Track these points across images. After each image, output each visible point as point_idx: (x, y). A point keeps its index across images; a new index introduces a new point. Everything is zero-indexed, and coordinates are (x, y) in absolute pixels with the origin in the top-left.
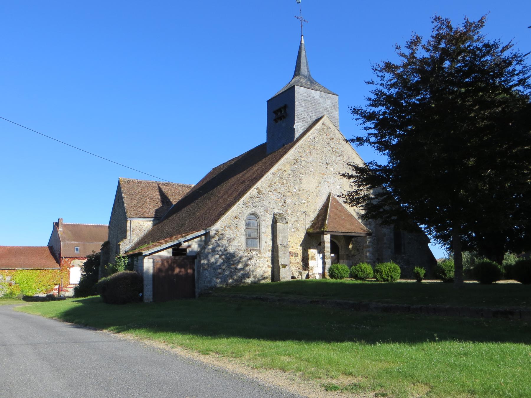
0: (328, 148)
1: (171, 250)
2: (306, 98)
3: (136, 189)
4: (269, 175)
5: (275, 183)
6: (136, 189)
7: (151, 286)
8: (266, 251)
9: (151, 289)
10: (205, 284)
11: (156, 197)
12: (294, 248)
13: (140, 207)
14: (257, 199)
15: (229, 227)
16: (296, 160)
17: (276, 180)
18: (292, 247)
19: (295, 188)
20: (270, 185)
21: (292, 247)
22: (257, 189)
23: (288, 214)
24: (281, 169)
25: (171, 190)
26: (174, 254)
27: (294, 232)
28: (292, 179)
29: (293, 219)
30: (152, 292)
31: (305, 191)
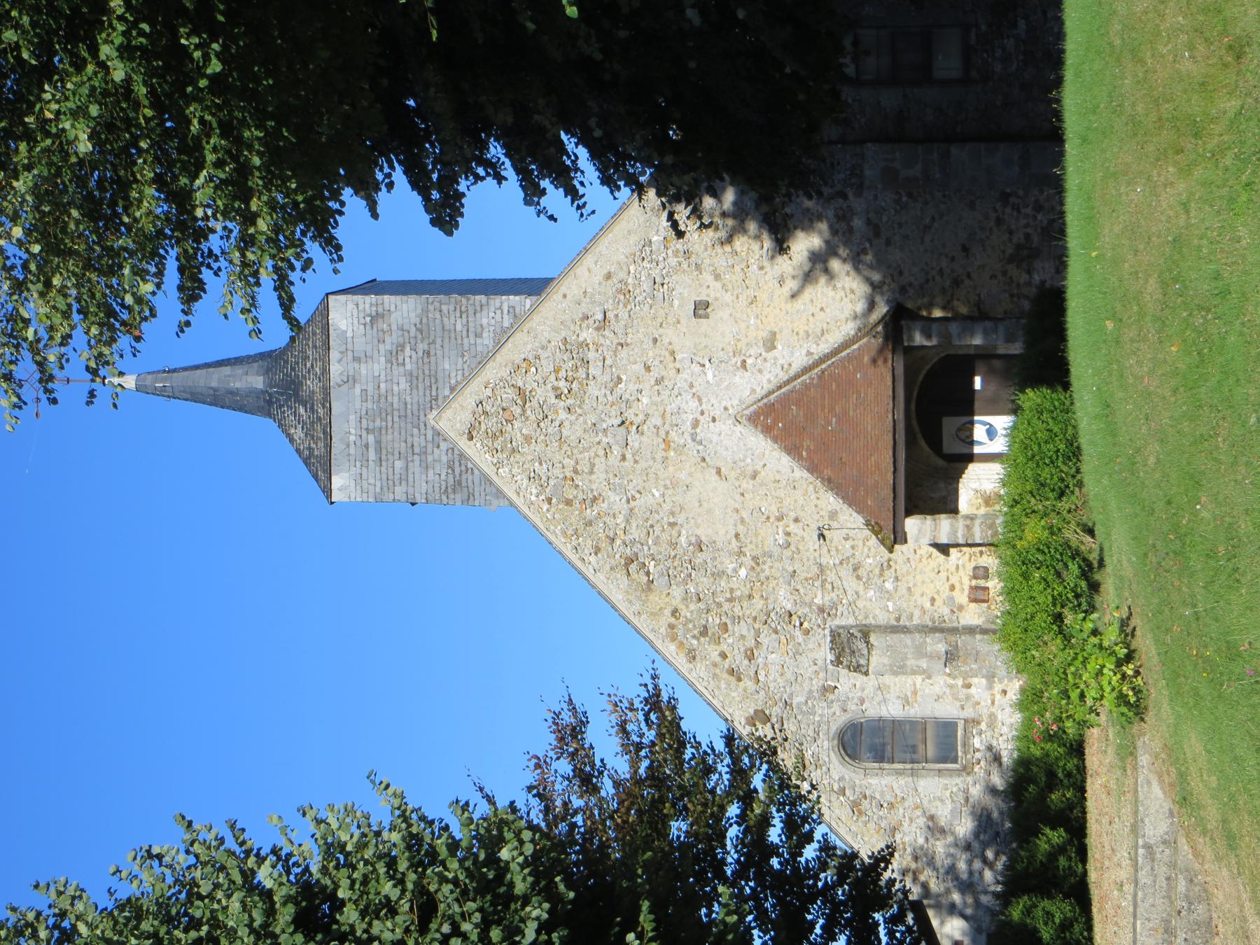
5: (724, 656)
8: (968, 697)
12: (954, 580)
16: (629, 561)
18: (952, 588)
21: (952, 588)
24: (671, 626)
27: (897, 579)
28: (703, 583)
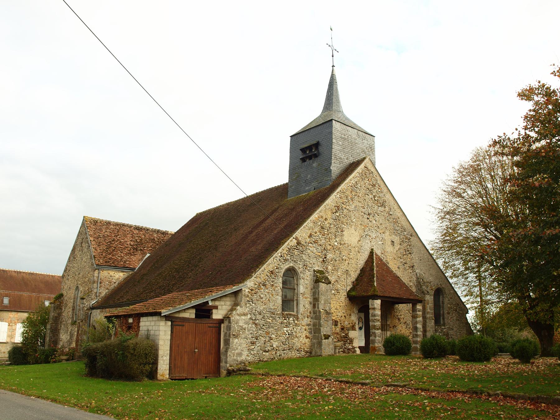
0: (371, 196)
1: (194, 311)
2: (343, 136)
3: (104, 231)
4: (309, 223)
5: (316, 233)
6: (104, 231)
7: (168, 357)
8: (304, 317)
9: (168, 361)
10: (235, 358)
11: (128, 243)
13: (110, 254)
14: (296, 252)
15: (264, 285)
16: (338, 207)
17: (317, 230)
19: (336, 241)
20: (310, 236)
22: (296, 239)
23: (328, 273)
25: (144, 235)
26: (197, 316)
28: (333, 230)
30: (168, 366)
31: (347, 245)
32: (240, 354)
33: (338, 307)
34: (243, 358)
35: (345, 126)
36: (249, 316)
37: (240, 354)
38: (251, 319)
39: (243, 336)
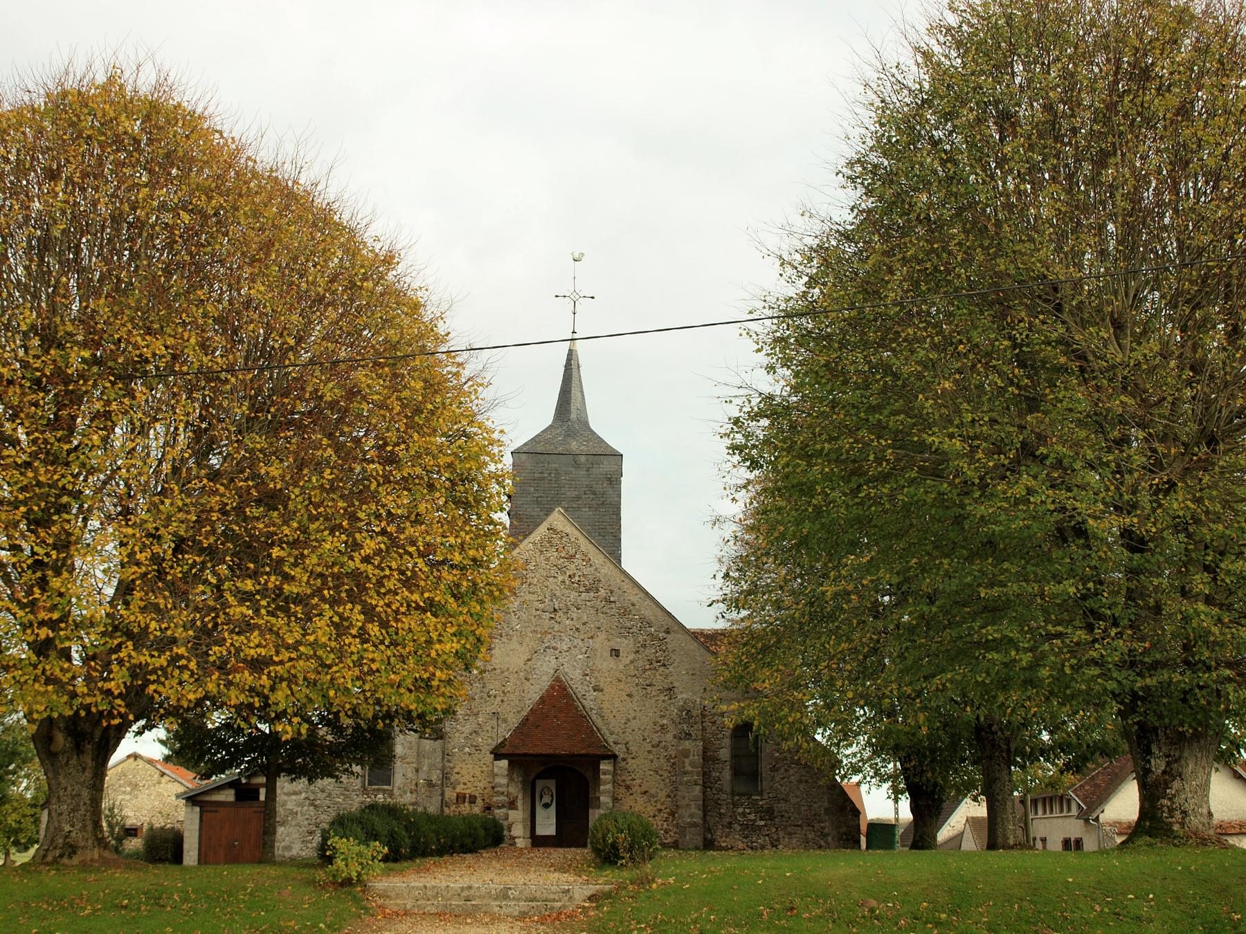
0: (560, 578)
1: (232, 792)
7: (196, 852)
8: (405, 792)
26: (239, 797)
29: (467, 729)
31: (498, 671)
32: (288, 848)
33: (478, 774)
34: (294, 852)
35: (542, 458)
36: (304, 795)
37: (288, 848)
38: (307, 798)
39: (294, 823)
